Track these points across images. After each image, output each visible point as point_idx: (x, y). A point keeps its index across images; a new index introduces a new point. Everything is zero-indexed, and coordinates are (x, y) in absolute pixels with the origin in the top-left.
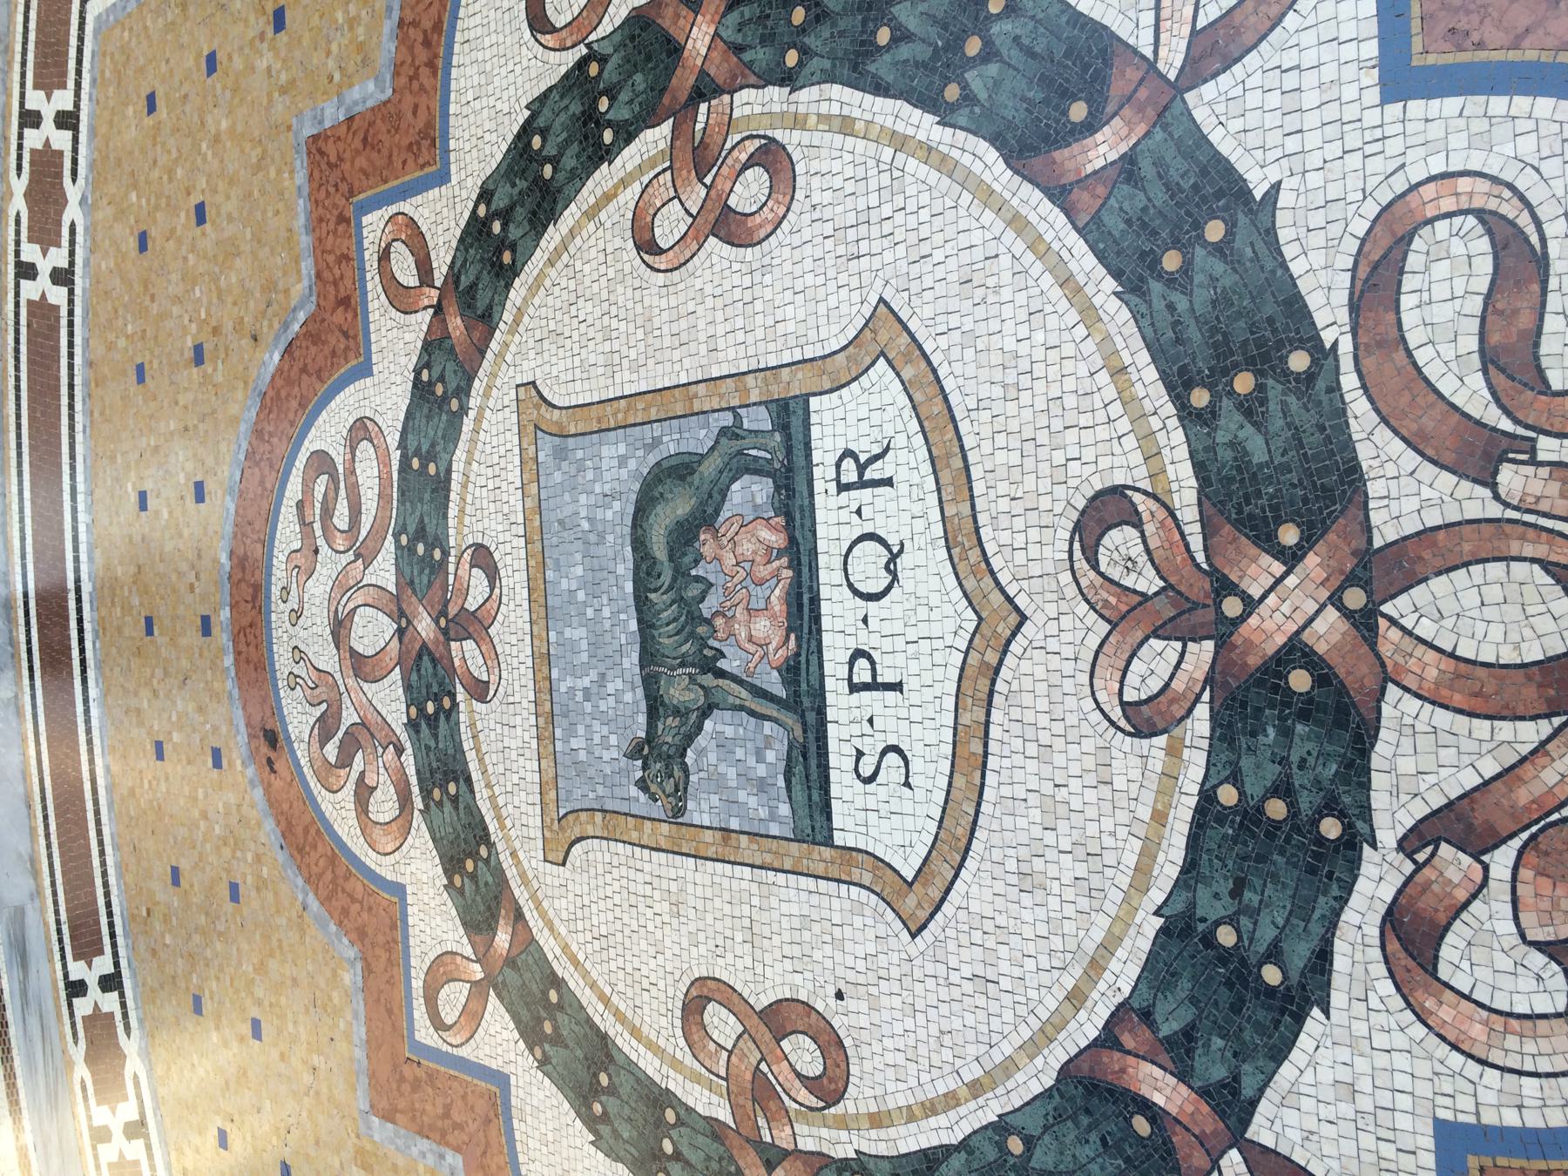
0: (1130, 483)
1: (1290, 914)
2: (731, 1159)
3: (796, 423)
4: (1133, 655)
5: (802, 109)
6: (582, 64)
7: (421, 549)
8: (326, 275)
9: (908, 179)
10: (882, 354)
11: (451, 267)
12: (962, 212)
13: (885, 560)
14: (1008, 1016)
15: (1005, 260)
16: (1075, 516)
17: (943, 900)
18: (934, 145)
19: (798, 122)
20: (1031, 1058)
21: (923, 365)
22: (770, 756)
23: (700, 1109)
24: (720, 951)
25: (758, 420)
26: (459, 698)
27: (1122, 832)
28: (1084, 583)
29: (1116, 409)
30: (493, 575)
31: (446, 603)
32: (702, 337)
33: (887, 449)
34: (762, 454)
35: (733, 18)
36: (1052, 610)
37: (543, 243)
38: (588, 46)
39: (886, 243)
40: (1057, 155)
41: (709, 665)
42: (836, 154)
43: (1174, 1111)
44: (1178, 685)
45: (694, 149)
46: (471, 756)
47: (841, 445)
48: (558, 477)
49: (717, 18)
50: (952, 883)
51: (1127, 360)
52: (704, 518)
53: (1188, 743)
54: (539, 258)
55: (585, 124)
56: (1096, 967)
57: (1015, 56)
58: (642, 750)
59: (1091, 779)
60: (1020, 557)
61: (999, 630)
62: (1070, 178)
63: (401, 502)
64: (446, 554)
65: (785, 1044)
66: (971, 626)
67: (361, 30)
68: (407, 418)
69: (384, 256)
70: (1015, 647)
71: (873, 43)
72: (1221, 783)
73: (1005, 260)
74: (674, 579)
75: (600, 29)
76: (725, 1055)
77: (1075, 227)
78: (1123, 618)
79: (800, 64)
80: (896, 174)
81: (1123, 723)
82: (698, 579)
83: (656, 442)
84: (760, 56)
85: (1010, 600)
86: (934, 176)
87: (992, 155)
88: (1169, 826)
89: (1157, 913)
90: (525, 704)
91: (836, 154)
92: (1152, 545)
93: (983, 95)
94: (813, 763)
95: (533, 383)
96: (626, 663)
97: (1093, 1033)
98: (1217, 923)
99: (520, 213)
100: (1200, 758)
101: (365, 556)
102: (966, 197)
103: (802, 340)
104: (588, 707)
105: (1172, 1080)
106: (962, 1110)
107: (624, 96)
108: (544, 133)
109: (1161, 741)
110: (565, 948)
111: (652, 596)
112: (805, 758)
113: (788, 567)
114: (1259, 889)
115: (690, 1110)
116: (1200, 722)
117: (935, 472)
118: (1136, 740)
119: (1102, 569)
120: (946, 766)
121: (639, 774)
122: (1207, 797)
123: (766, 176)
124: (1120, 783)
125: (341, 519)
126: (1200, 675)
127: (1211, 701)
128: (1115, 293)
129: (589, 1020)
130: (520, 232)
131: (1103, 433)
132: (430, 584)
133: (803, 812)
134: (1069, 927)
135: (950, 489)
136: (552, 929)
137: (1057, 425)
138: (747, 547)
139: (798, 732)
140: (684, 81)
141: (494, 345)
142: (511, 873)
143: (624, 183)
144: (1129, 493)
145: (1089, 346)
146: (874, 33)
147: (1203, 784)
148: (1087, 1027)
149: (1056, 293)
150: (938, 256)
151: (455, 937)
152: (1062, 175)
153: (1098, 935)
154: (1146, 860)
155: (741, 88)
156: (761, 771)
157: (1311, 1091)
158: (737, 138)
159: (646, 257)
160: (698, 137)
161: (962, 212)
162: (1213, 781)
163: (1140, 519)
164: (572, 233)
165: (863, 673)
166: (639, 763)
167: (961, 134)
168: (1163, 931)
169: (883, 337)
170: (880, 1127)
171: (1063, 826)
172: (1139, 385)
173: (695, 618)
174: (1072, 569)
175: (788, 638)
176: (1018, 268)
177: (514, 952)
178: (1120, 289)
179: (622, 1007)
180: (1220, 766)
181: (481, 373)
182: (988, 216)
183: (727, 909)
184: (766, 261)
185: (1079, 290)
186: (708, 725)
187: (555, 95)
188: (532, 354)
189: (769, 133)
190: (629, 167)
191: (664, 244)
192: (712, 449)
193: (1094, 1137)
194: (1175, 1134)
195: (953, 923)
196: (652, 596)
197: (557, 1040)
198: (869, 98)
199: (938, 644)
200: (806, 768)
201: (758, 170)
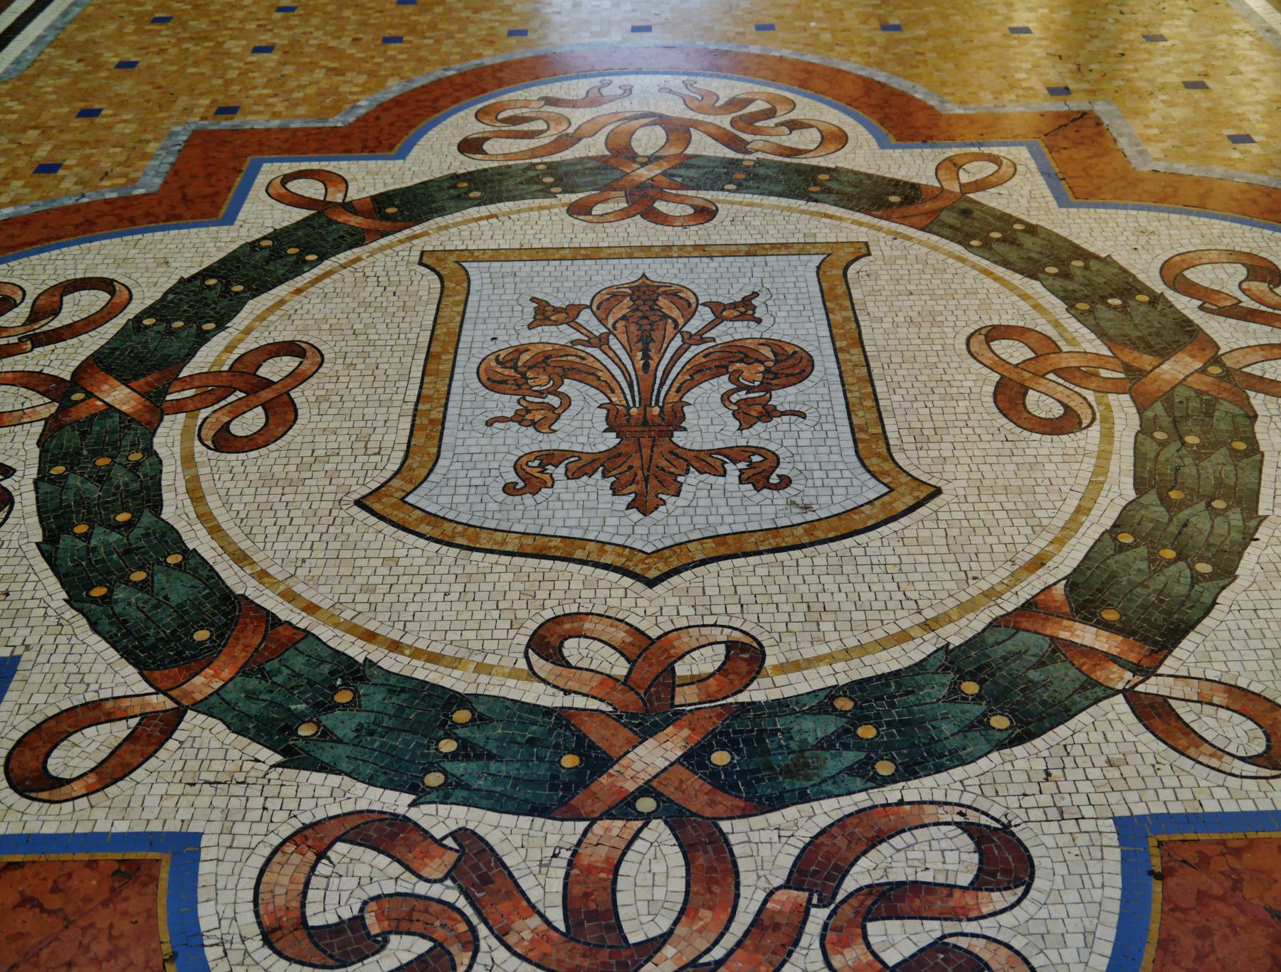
65: (260, 410)
95: (869, 254)
128: (948, 644)
158: (1090, 396)
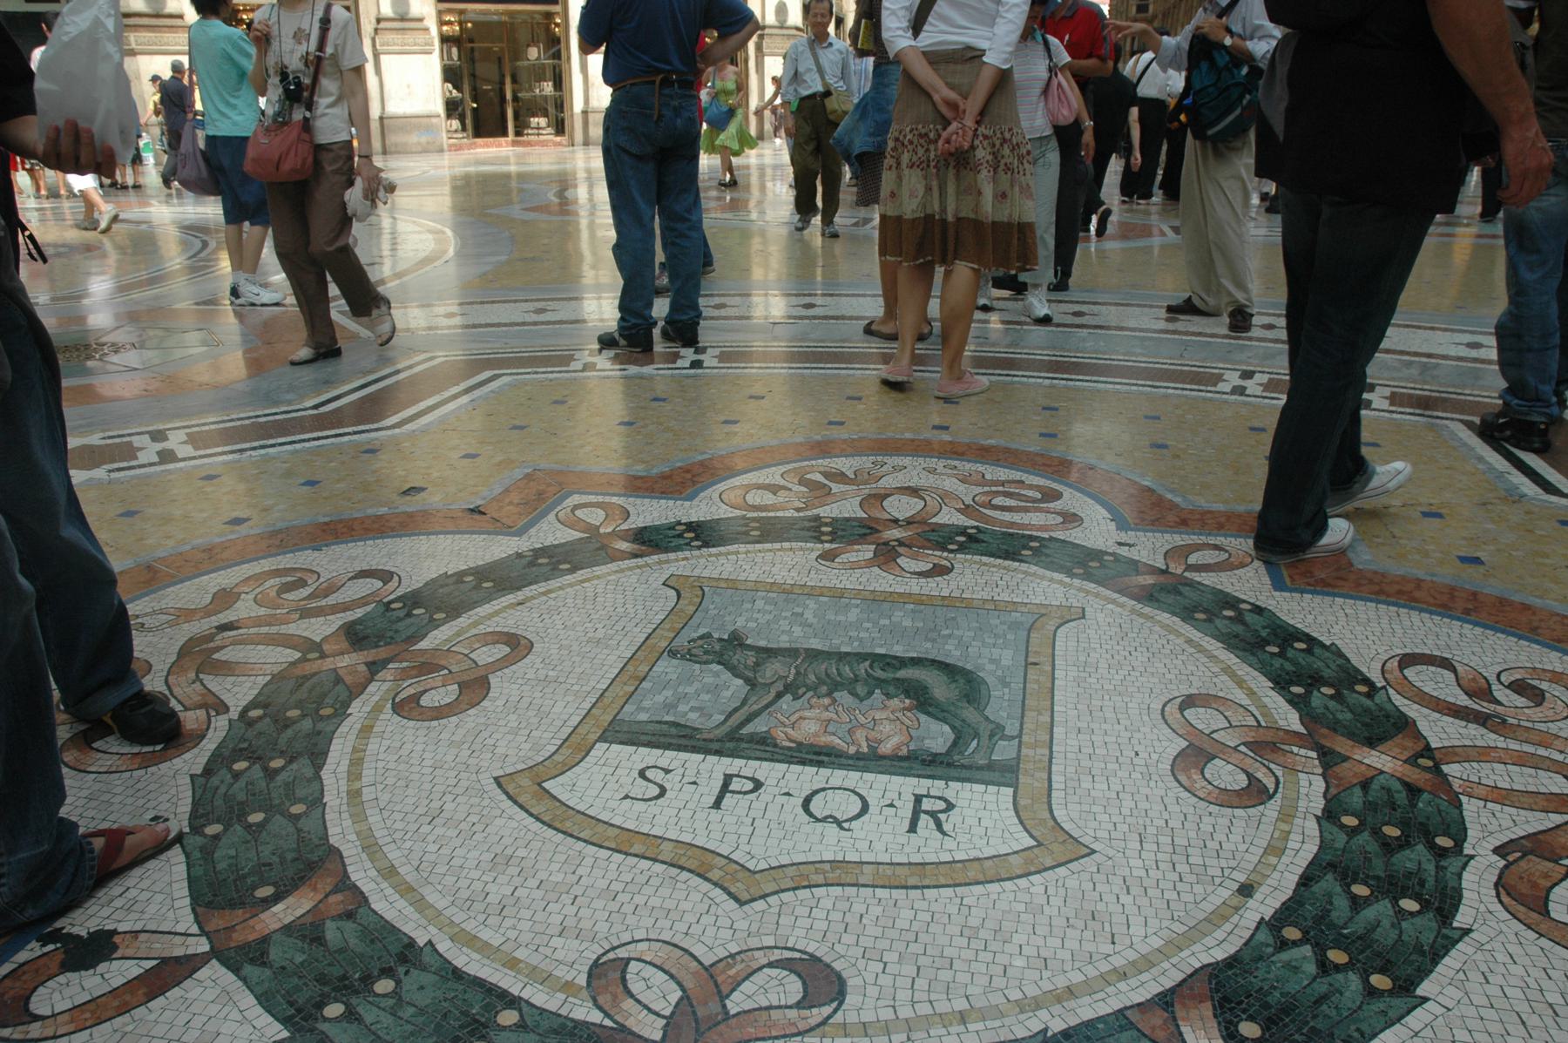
0: (843, 1007)
1: (379, 1037)
2: (387, 644)
3: (996, 776)
4: (672, 976)
5: (1297, 821)
6: (1367, 681)
7: (962, 539)
8: (1209, 516)
9: (1210, 889)
10: (1040, 844)
11: (1199, 583)
12: (1166, 923)
13: (839, 816)
14: (399, 825)
15: (1108, 949)
16: (827, 959)
17: (515, 802)
18: (1240, 912)
19: (1286, 816)
20: (358, 834)
21: (1019, 872)
22: (693, 716)
23: (435, 632)
24: (547, 661)
25: (1004, 751)
26: (827, 546)
27: (512, 934)
28: (757, 954)
29: (924, 1009)
30: (921, 574)
31: (910, 547)
32: (1094, 726)
33: (944, 833)
34: (970, 750)
35: (1397, 786)
36: (739, 925)
37: (1207, 638)
38: (1384, 687)
39: (1151, 864)
40: (1209, 1004)
41: (790, 689)
42: (1248, 840)
43: (262, 916)
44: (628, 1004)
45: (1274, 744)
46: (777, 546)
47: (960, 803)
48: (995, 622)
49: (1398, 775)
50: (527, 811)
51: (971, 1027)
52: (922, 700)
53: (570, 999)
54: (1195, 635)
55: (1310, 677)
56: (406, 890)
57: (1321, 987)
58: (736, 641)
59: (570, 922)
60: (801, 911)
61: (739, 884)
62: (1180, 1012)
63: (1004, 533)
64: (952, 551)
65: (456, 686)
66: (751, 865)
67: (1417, 557)
68: (1078, 545)
69: (1217, 547)
70: (718, 891)
71: (1355, 881)
72: (521, 1016)
73: (1108, 949)
74: (877, 679)
75: (1399, 697)
76: (466, 652)
77: (1126, 1008)
78: (712, 977)
79: (1342, 827)
80: (1218, 881)
81: (611, 956)
82: (870, 693)
83: (1006, 685)
84: (1356, 798)
85: (764, 897)
86: (1208, 907)
87: (1219, 954)
88: (501, 968)
89: (430, 942)
90: (805, 579)
91: (1248, 840)
92: (775, 1014)
93: (1285, 956)
94: (674, 741)
95: (1084, 617)
96: (812, 640)
97: (354, 877)
98: (398, 982)
99: (1239, 629)
100: (552, 1006)
101: (966, 510)
102: (1181, 929)
103: (1071, 791)
104: (788, 614)
105: (286, 921)
106: (343, 782)
107: (1332, 704)
108: (1309, 651)
109: (582, 980)
110: (598, 577)
111: (867, 663)
112: (684, 736)
113: (857, 752)
114: (413, 1019)
115: (437, 627)
116: (584, 1012)
117: (910, 864)
118: (591, 962)
119: (765, 970)
120: (630, 825)
121: (716, 635)
122: (513, 1002)
123: (1237, 788)
124: (556, 942)
125: (998, 501)
126: (631, 1023)
127: (601, 1026)
128: (1046, 1030)
129: (536, 583)
130: (1219, 626)
131: (904, 995)
132: (929, 540)
133: (635, 728)
134: (449, 880)
135: (889, 872)
136: (616, 572)
137: (922, 961)
138: (887, 728)
139: (706, 736)
140: (1341, 745)
141: (1124, 599)
142: (672, 556)
143: (1251, 693)
144: (835, 1005)
145: (997, 999)
146: (1366, 884)
147: (527, 1002)
148: (362, 874)
149: (1061, 982)
150: (1124, 899)
151: (637, 522)
152: (1184, 1005)
153: (432, 897)
154: (479, 944)
155: (1326, 782)
156: (683, 708)
157: (222, 1015)
158: (1279, 773)
159: (1180, 700)
160: (1286, 747)
161: (1166, 923)
162: (525, 1009)
163: (804, 1008)
164: (1211, 657)
165: (736, 785)
166: (726, 637)
167: (1247, 934)
168: (411, 943)
169: (1055, 847)
170: (361, 731)
171: (538, 894)
172: (944, 1031)
173: (835, 686)
174: (776, 947)
175: (791, 741)
176: (1095, 957)
177: (609, 551)
178: (1050, 1034)
179: (536, 601)
180: (538, 1018)
181: (1101, 589)
182: (1157, 942)
183: (579, 670)
184: (1155, 777)
185: (1059, 1000)
186: (740, 682)
187: (1340, 661)
188: (1108, 620)
189: (1279, 795)
190: (1266, 700)
191: (1186, 713)
192: (987, 718)
193: (275, 859)
194: (244, 913)
195: (493, 804)
196: (867, 663)
197: (532, 564)
198: (1300, 871)
199: (744, 839)
200: (671, 736)
201: (1244, 783)
